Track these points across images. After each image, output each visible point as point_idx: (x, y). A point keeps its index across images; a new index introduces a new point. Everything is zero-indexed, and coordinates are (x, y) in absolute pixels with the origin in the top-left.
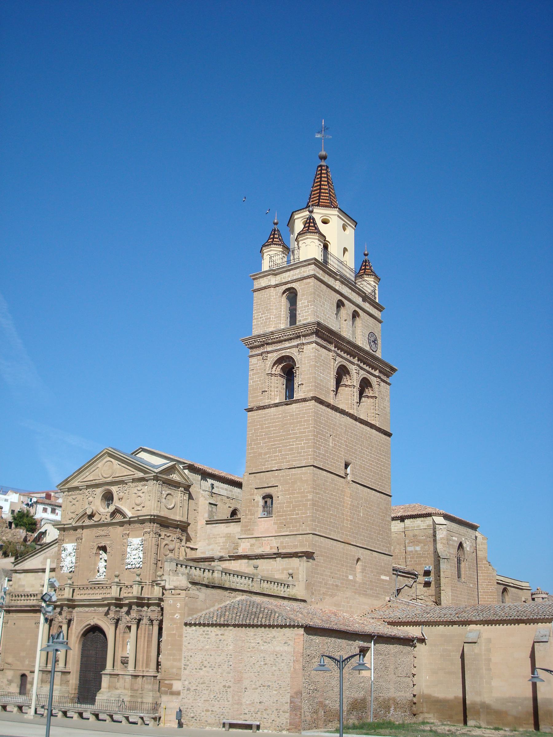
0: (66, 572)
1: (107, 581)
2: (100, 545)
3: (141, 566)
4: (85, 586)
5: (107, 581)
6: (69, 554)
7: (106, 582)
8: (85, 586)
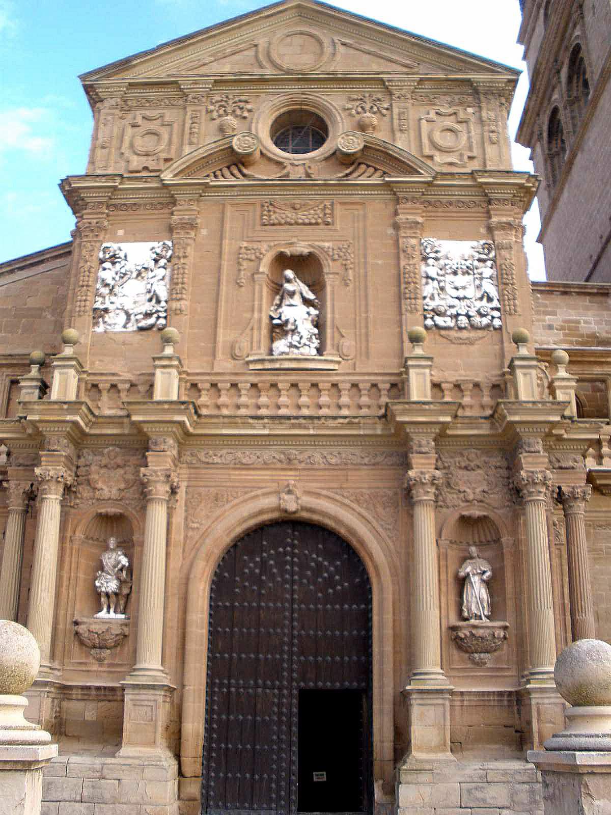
0: (119, 328)
1: (339, 363)
2: (288, 251)
3: (497, 323)
4: (227, 378)
5: (339, 363)
6: (139, 274)
7: (336, 367)
8: (227, 378)
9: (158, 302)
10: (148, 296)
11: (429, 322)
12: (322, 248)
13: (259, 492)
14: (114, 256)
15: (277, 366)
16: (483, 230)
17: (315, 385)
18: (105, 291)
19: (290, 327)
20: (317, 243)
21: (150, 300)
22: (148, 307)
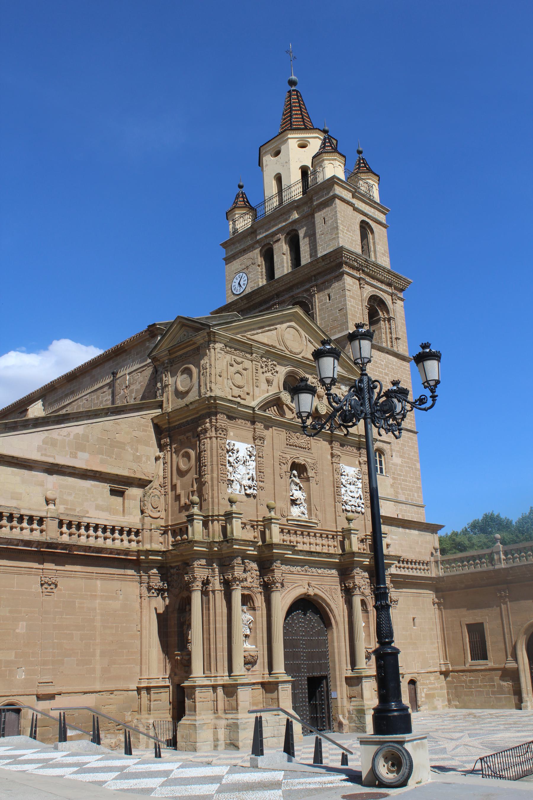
9: (253, 480)
10: (248, 476)
11: (343, 507)
12: (308, 462)
13: (296, 585)
14: (232, 449)
15: (299, 523)
16: (357, 463)
17: (309, 533)
18: (231, 469)
19: (298, 502)
20: (308, 460)
21: (249, 479)
22: (250, 483)
